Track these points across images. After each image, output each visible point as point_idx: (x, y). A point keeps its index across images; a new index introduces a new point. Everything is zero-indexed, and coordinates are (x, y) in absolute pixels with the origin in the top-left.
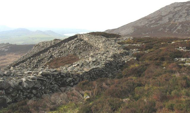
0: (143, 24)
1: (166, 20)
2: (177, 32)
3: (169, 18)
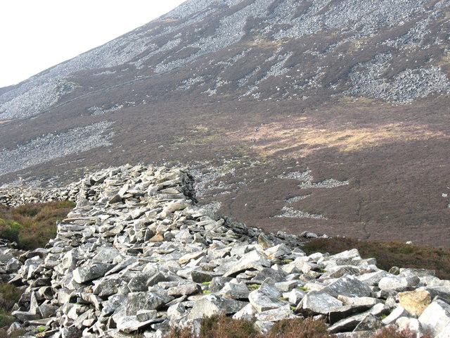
0: (123, 59)
1: (233, 30)
2: (257, 96)
3: (250, 20)
